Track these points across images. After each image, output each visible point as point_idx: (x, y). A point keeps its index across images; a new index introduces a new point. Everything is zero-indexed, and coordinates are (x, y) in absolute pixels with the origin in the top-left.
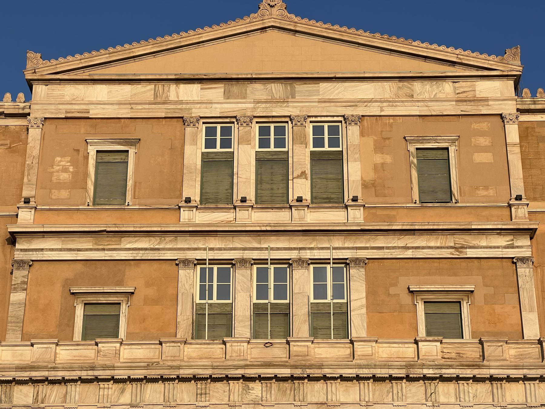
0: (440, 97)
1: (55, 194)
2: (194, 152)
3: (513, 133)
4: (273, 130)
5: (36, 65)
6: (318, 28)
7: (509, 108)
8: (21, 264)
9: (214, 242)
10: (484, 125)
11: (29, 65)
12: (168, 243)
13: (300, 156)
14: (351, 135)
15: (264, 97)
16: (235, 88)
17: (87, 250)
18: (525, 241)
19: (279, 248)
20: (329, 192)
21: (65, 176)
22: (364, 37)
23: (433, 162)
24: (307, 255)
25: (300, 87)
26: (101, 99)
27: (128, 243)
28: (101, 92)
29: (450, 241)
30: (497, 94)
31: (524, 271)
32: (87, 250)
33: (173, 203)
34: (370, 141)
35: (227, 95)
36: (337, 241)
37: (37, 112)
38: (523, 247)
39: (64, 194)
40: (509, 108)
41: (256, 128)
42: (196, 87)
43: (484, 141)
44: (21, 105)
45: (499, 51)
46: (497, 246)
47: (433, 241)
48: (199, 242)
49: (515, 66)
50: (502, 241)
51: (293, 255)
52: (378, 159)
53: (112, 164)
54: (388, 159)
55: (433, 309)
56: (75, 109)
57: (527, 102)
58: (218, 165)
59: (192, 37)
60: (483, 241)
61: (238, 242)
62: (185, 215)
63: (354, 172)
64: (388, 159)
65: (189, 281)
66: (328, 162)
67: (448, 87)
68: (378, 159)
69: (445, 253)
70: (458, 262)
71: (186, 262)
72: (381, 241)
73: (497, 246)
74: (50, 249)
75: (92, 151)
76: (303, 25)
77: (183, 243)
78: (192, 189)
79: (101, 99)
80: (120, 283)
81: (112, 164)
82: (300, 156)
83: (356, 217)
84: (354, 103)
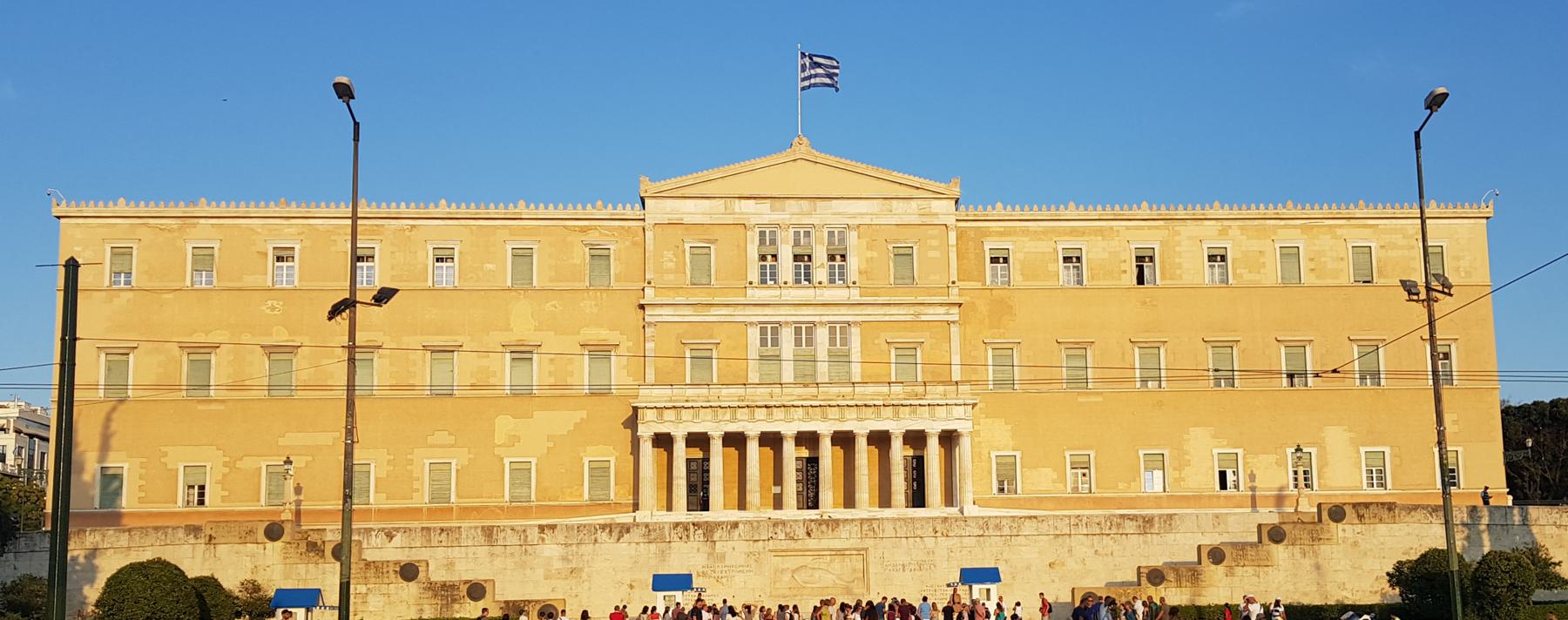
0: (907, 212)
1: (666, 277)
2: (753, 251)
3: (953, 236)
4: (803, 234)
5: (647, 187)
6: (832, 160)
7: (951, 221)
8: (650, 324)
9: (768, 311)
10: (935, 231)
11: (643, 187)
12: (739, 311)
13: (820, 255)
14: (852, 237)
15: (796, 210)
16: (778, 203)
17: (689, 315)
18: (955, 310)
19: (807, 315)
20: (838, 275)
21: (671, 265)
22: (861, 167)
23: (904, 256)
24: (825, 319)
25: (819, 203)
26: (691, 211)
27: (714, 311)
28: (690, 205)
29: (912, 310)
30: (944, 210)
31: (954, 328)
32: (689, 315)
33: (742, 284)
34: (864, 242)
35: (773, 209)
36: (843, 310)
37: (649, 221)
38: (954, 314)
39: (672, 277)
40: (951, 221)
41: (792, 231)
42: (752, 202)
43: (934, 243)
44: (638, 213)
45: (946, 180)
46: (939, 314)
47: (902, 310)
48: (758, 310)
49: (956, 191)
50: (942, 310)
51: (817, 319)
52: (869, 254)
53: (701, 255)
54: (875, 254)
55: (900, 352)
56: (674, 218)
57: (962, 214)
58: (768, 258)
59: (747, 165)
60: (931, 310)
61: (783, 310)
62: (749, 291)
63: (853, 263)
64: (875, 254)
65: (754, 334)
66: (837, 256)
67: (914, 203)
68: (869, 254)
69: (908, 318)
70: (916, 324)
71: (751, 324)
72: (870, 310)
73: (939, 314)
74: (666, 314)
75: (687, 246)
76: (821, 157)
77: (749, 311)
78: (754, 275)
79: (691, 211)
80: (711, 337)
81: (701, 255)
82: (820, 255)
83: (855, 295)
84: (854, 216)
